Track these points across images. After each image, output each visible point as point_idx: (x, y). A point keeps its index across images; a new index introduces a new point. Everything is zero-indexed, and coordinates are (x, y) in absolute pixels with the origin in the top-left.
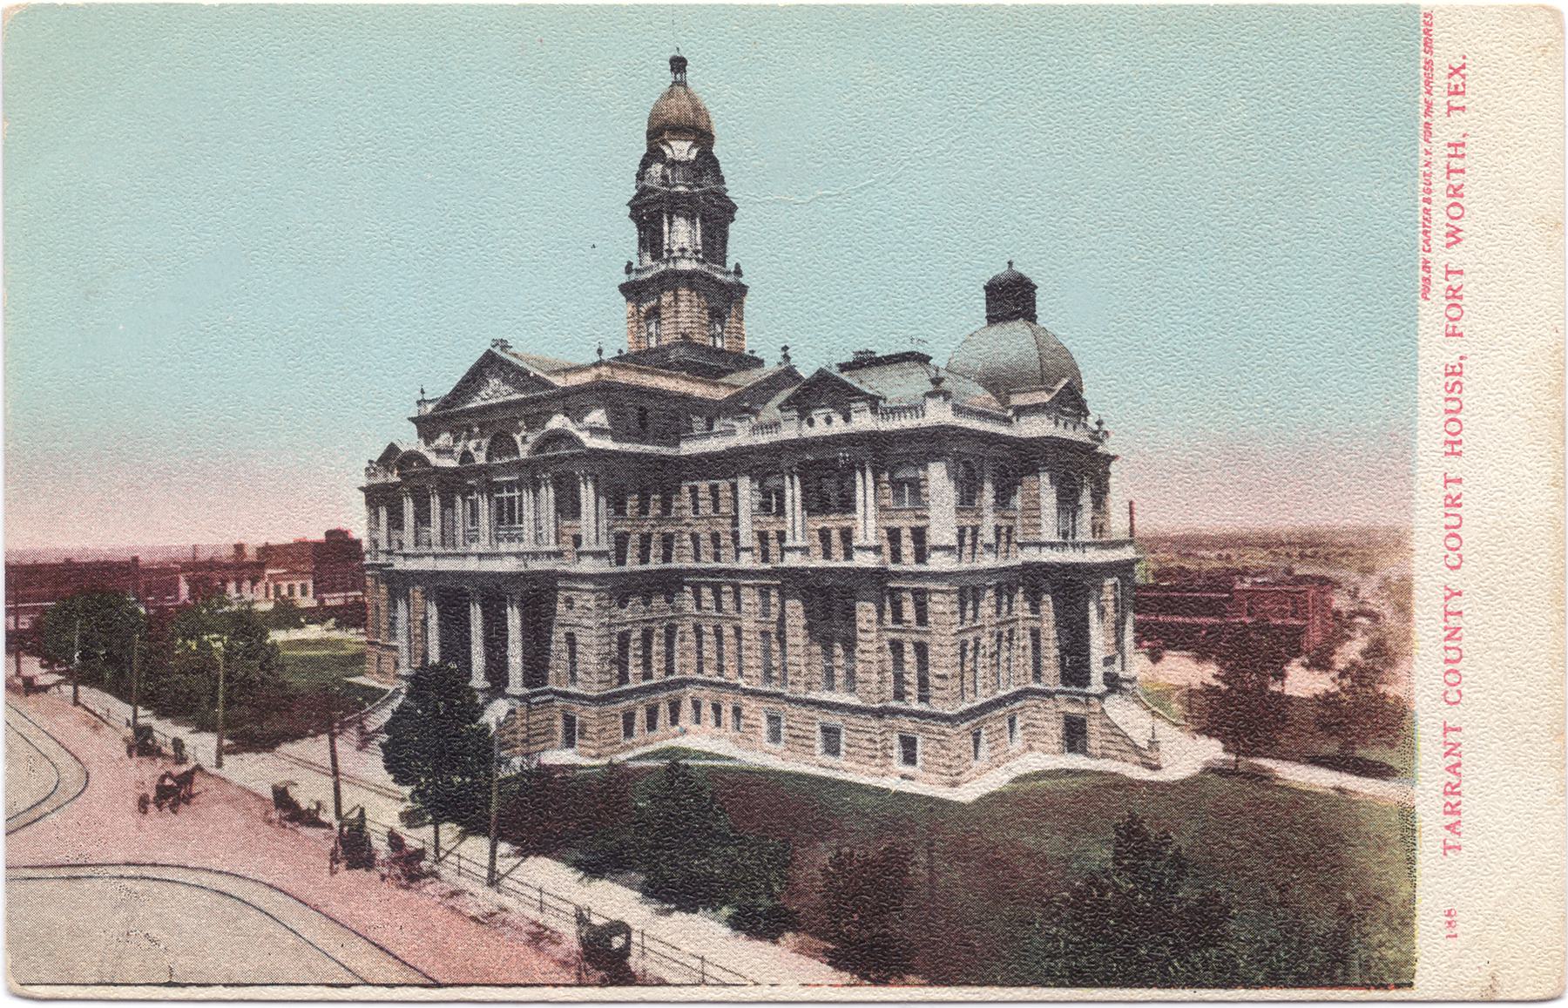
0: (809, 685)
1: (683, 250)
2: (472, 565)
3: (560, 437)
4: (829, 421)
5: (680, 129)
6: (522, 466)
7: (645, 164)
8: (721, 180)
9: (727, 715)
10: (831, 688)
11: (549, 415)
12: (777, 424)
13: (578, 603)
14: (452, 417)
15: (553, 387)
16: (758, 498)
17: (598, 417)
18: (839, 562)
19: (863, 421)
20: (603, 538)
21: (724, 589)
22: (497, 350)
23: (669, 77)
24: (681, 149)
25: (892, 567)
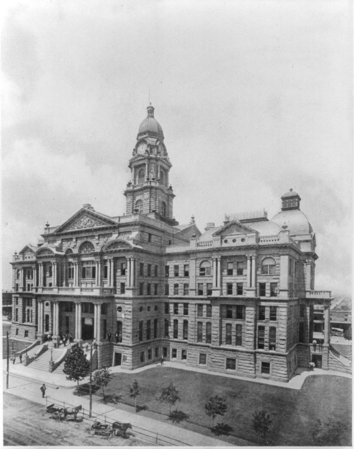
0: (221, 343)
1: (153, 179)
2: (77, 292)
3: (115, 244)
4: (234, 241)
5: (152, 133)
6: (95, 254)
7: (137, 145)
8: (166, 154)
9: (179, 354)
10: (230, 343)
11: (110, 235)
12: (211, 242)
13: (123, 309)
14: (63, 234)
15: (114, 223)
16: (198, 272)
17: (134, 234)
18: (234, 295)
19: (251, 241)
20: (136, 284)
21: (179, 305)
22: (86, 209)
23: (145, 114)
24: (152, 141)
25: (262, 298)
